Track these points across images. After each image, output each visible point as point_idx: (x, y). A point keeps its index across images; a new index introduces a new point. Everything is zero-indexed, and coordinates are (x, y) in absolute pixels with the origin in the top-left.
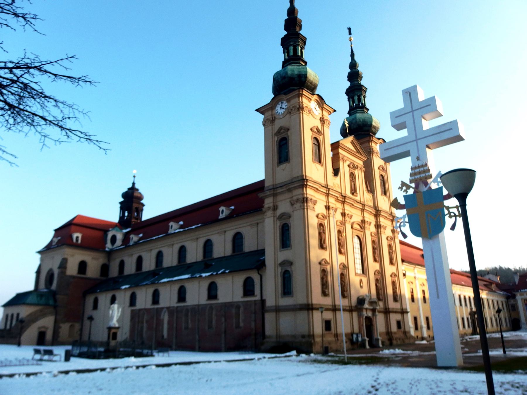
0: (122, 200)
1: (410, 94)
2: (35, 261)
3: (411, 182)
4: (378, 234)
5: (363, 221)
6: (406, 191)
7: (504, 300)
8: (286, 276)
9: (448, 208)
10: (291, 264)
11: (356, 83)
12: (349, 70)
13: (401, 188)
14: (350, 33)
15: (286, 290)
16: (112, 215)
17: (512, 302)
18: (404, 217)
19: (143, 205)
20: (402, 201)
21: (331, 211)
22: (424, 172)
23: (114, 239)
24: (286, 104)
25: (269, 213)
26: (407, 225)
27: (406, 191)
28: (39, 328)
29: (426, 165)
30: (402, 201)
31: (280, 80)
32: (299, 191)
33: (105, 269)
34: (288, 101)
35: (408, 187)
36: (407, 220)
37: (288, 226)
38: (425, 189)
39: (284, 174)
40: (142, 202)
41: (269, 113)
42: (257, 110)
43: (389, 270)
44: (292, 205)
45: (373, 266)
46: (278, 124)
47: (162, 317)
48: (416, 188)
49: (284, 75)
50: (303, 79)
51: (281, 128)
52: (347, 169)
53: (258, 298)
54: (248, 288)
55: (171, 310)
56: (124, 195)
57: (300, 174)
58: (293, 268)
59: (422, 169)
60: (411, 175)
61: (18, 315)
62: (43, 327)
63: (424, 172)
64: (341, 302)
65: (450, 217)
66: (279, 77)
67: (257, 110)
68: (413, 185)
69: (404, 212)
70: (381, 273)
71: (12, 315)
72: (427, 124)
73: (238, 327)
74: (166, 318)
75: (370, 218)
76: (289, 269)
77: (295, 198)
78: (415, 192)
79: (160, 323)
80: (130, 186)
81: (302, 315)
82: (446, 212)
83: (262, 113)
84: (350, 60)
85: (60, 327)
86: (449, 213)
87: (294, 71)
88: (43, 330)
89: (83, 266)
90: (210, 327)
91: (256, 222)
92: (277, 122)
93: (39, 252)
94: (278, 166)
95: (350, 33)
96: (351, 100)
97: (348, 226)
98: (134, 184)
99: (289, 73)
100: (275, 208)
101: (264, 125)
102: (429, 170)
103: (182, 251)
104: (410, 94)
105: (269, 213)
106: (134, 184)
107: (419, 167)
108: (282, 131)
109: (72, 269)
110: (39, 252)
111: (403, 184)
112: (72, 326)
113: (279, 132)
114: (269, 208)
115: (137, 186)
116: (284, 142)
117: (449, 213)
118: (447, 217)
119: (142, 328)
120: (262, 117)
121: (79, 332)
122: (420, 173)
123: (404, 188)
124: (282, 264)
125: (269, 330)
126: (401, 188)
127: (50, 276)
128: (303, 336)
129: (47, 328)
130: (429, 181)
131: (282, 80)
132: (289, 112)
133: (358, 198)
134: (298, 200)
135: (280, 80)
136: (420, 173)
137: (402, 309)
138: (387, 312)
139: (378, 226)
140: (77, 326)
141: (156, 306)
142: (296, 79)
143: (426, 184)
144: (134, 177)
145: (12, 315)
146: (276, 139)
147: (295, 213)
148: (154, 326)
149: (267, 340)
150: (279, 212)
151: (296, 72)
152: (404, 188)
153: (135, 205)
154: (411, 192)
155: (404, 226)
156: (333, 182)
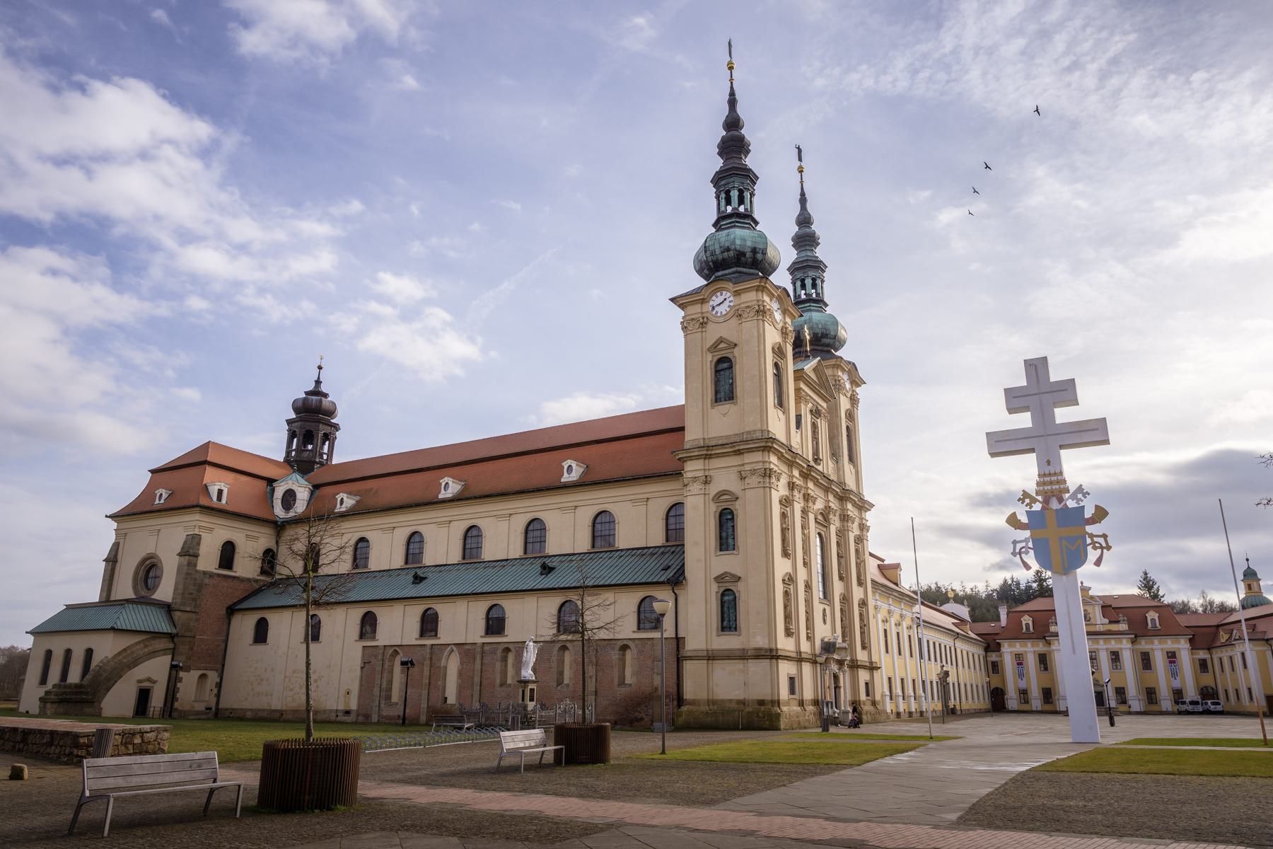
0: (293, 416)
1: (1036, 367)
2: (107, 534)
3: (1037, 494)
4: (842, 533)
5: (828, 508)
6: (1029, 505)
7: (982, 652)
8: (726, 598)
9: (1092, 536)
12: (797, 228)
13: (1022, 500)
14: (800, 159)
16: (268, 441)
17: (993, 657)
18: (1026, 540)
19: (336, 427)
20: (1024, 519)
21: (796, 492)
22: (1058, 482)
23: (289, 498)
25: (696, 488)
26: (1032, 552)
27: (1029, 505)
28: (139, 681)
29: (1061, 473)
30: (1024, 519)
32: (758, 456)
33: (269, 558)
34: (737, 293)
35: (1034, 500)
36: (1030, 545)
37: (732, 513)
38: (1059, 507)
39: (721, 423)
41: (695, 310)
42: (672, 300)
43: (857, 593)
44: (743, 478)
45: (838, 588)
47: (443, 662)
48: (1046, 502)
51: (721, 340)
52: (809, 416)
53: (669, 631)
54: (648, 618)
55: (465, 650)
57: (759, 426)
60: (1038, 484)
61: (89, 652)
62: (149, 680)
63: (1058, 482)
64: (805, 647)
65: (1095, 548)
66: (717, 246)
67: (672, 300)
68: (1040, 498)
69: (1027, 534)
70: (846, 599)
71: (68, 653)
72: (1063, 415)
73: (622, 683)
74: (453, 666)
75: (834, 504)
77: (747, 468)
78: (1043, 508)
79: (437, 674)
80: (311, 387)
81: (757, 668)
82: (1089, 541)
83: (682, 306)
84: (797, 209)
85: (181, 680)
86: (1093, 543)
87: (745, 240)
88: (146, 684)
89: (228, 552)
90: (560, 682)
92: (710, 326)
93: (113, 517)
94: (713, 407)
95: (800, 159)
96: (798, 284)
97: (811, 516)
98: (318, 382)
99: (738, 242)
101: (684, 328)
102: (1065, 481)
103: (472, 536)
104: (1036, 367)
105: (696, 488)
106: (318, 382)
108: (722, 345)
109: (208, 560)
110: (113, 517)
111: (1026, 494)
112: (203, 676)
113: (714, 348)
114: (695, 479)
115: (324, 388)
116: (725, 365)
117: (1093, 543)
118: (1089, 548)
119: (390, 682)
120: (682, 313)
121: (215, 691)
122: (1051, 483)
123: (1027, 501)
124: (720, 579)
125: (691, 690)
126: (1022, 500)
127: (149, 571)
128: (761, 703)
129: (154, 682)
130: (1067, 495)
133: (820, 468)
134: (753, 472)
136: (1051, 483)
137: (871, 663)
138: (855, 666)
139: (845, 518)
140: (213, 677)
141: (428, 642)
142: (748, 255)
143: (1060, 500)
144: (320, 368)
145: (68, 653)
146: (709, 357)
148: (426, 681)
149: (684, 709)
150: (713, 489)
151: (749, 244)
152: (1027, 501)
153: (323, 429)
154: (1037, 507)
155: (1027, 553)
156: (795, 441)
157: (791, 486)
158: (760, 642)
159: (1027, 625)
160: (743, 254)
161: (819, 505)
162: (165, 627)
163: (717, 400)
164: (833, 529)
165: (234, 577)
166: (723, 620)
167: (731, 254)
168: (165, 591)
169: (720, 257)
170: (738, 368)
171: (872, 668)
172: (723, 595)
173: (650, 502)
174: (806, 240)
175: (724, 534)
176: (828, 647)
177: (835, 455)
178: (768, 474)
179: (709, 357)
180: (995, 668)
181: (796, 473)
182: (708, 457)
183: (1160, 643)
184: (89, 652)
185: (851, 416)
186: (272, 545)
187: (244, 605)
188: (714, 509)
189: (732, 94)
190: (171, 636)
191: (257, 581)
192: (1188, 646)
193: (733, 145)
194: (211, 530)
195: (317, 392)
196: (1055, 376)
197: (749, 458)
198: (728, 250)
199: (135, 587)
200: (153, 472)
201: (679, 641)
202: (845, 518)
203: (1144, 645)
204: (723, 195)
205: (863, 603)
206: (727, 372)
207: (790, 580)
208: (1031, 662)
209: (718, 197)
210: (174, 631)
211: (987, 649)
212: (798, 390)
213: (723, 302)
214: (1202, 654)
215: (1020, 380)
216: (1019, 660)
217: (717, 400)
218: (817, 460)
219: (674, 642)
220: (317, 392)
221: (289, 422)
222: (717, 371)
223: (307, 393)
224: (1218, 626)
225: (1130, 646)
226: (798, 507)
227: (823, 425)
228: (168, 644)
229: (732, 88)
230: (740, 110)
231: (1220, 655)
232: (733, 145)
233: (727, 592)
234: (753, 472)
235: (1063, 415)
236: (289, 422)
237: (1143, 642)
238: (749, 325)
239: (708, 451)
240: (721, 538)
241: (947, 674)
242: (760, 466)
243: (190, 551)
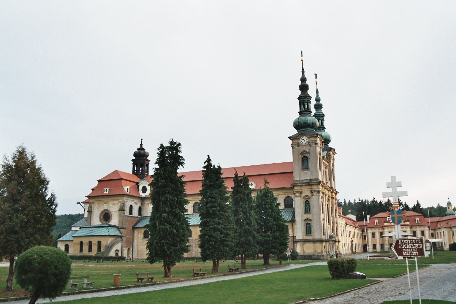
1: (393, 178)
7: (361, 232)
8: (307, 225)
10: (311, 220)
11: (320, 111)
14: (316, 78)
15: (307, 232)
19: (149, 161)
24: (307, 139)
31: (302, 123)
32: (316, 187)
34: (309, 138)
37: (308, 201)
40: (148, 158)
45: (331, 219)
46: (301, 149)
49: (305, 121)
50: (314, 125)
51: (304, 151)
56: (135, 155)
58: (312, 222)
59: (396, 204)
66: (302, 122)
76: (310, 223)
80: (139, 147)
88: (117, 252)
91: (278, 194)
92: (300, 147)
95: (316, 78)
98: (141, 145)
99: (308, 121)
100: (301, 193)
101: (292, 147)
104: (393, 178)
106: (141, 145)
107: (395, 203)
108: (304, 153)
113: (301, 154)
114: (298, 192)
115: (144, 147)
116: (306, 158)
120: (291, 141)
122: (396, 205)
124: (305, 220)
131: (304, 124)
132: (309, 144)
133: (327, 184)
134: (315, 191)
135: (302, 123)
136: (396, 205)
139: (332, 198)
144: (142, 139)
147: (314, 197)
150: (303, 195)
151: (311, 122)
153: (146, 162)
157: (323, 193)
158: (317, 237)
159: (377, 222)
160: (310, 124)
161: (327, 197)
162: (120, 235)
163: (303, 169)
164: (330, 202)
165: (133, 217)
166: (307, 231)
167: (306, 124)
168: (114, 221)
169: (303, 125)
170: (309, 161)
171: (339, 242)
172: (306, 224)
173: (280, 196)
174: (318, 107)
175: (306, 208)
176: (331, 237)
177: (330, 180)
178: (319, 192)
179: (300, 156)
180: (364, 238)
181: (324, 188)
182: (301, 186)
183: (419, 228)
184: (99, 243)
185: (333, 165)
186: (141, 206)
187: (138, 226)
188: (304, 201)
189: (303, 69)
190: (121, 237)
191: (138, 217)
192: (428, 229)
193: (304, 88)
194: (127, 202)
195: (141, 149)
196: (397, 181)
197: (313, 187)
198: (305, 123)
199: (101, 221)
200: (98, 181)
201: (294, 237)
202: (332, 198)
203: (414, 229)
204: (302, 104)
205: (337, 223)
206: (306, 161)
207: (324, 220)
208: (377, 235)
209: (300, 103)
210: (122, 235)
211: (363, 231)
212: (323, 162)
213: (304, 140)
214: (432, 232)
215: (390, 181)
216: (373, 235)
217: (303, 169)
218: (327, 183)
219: (292, 238)
220: (141, 149)
221: (133, 160)
222: (303, 160)
223: (138, 149)
224: (438, 222)
225: (410, 229)
226: (324, 198)
227: (327, 170)
228: (120, 239)
229: (303, 67)
230: (306, 75)
231: (438, 232)
232: (304, 88)
233: (308, 223)
234: (315, 191)
235: (399, 189)
236: (133, 160)
237: (414, 228)
238: (312, 148)
239: (302, 184)
240: (305, 209)
241: (353, 241)
242: (317, 189)
243: (122, 209)
